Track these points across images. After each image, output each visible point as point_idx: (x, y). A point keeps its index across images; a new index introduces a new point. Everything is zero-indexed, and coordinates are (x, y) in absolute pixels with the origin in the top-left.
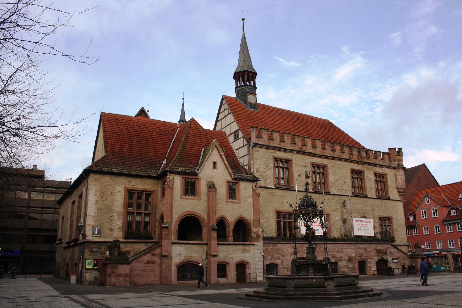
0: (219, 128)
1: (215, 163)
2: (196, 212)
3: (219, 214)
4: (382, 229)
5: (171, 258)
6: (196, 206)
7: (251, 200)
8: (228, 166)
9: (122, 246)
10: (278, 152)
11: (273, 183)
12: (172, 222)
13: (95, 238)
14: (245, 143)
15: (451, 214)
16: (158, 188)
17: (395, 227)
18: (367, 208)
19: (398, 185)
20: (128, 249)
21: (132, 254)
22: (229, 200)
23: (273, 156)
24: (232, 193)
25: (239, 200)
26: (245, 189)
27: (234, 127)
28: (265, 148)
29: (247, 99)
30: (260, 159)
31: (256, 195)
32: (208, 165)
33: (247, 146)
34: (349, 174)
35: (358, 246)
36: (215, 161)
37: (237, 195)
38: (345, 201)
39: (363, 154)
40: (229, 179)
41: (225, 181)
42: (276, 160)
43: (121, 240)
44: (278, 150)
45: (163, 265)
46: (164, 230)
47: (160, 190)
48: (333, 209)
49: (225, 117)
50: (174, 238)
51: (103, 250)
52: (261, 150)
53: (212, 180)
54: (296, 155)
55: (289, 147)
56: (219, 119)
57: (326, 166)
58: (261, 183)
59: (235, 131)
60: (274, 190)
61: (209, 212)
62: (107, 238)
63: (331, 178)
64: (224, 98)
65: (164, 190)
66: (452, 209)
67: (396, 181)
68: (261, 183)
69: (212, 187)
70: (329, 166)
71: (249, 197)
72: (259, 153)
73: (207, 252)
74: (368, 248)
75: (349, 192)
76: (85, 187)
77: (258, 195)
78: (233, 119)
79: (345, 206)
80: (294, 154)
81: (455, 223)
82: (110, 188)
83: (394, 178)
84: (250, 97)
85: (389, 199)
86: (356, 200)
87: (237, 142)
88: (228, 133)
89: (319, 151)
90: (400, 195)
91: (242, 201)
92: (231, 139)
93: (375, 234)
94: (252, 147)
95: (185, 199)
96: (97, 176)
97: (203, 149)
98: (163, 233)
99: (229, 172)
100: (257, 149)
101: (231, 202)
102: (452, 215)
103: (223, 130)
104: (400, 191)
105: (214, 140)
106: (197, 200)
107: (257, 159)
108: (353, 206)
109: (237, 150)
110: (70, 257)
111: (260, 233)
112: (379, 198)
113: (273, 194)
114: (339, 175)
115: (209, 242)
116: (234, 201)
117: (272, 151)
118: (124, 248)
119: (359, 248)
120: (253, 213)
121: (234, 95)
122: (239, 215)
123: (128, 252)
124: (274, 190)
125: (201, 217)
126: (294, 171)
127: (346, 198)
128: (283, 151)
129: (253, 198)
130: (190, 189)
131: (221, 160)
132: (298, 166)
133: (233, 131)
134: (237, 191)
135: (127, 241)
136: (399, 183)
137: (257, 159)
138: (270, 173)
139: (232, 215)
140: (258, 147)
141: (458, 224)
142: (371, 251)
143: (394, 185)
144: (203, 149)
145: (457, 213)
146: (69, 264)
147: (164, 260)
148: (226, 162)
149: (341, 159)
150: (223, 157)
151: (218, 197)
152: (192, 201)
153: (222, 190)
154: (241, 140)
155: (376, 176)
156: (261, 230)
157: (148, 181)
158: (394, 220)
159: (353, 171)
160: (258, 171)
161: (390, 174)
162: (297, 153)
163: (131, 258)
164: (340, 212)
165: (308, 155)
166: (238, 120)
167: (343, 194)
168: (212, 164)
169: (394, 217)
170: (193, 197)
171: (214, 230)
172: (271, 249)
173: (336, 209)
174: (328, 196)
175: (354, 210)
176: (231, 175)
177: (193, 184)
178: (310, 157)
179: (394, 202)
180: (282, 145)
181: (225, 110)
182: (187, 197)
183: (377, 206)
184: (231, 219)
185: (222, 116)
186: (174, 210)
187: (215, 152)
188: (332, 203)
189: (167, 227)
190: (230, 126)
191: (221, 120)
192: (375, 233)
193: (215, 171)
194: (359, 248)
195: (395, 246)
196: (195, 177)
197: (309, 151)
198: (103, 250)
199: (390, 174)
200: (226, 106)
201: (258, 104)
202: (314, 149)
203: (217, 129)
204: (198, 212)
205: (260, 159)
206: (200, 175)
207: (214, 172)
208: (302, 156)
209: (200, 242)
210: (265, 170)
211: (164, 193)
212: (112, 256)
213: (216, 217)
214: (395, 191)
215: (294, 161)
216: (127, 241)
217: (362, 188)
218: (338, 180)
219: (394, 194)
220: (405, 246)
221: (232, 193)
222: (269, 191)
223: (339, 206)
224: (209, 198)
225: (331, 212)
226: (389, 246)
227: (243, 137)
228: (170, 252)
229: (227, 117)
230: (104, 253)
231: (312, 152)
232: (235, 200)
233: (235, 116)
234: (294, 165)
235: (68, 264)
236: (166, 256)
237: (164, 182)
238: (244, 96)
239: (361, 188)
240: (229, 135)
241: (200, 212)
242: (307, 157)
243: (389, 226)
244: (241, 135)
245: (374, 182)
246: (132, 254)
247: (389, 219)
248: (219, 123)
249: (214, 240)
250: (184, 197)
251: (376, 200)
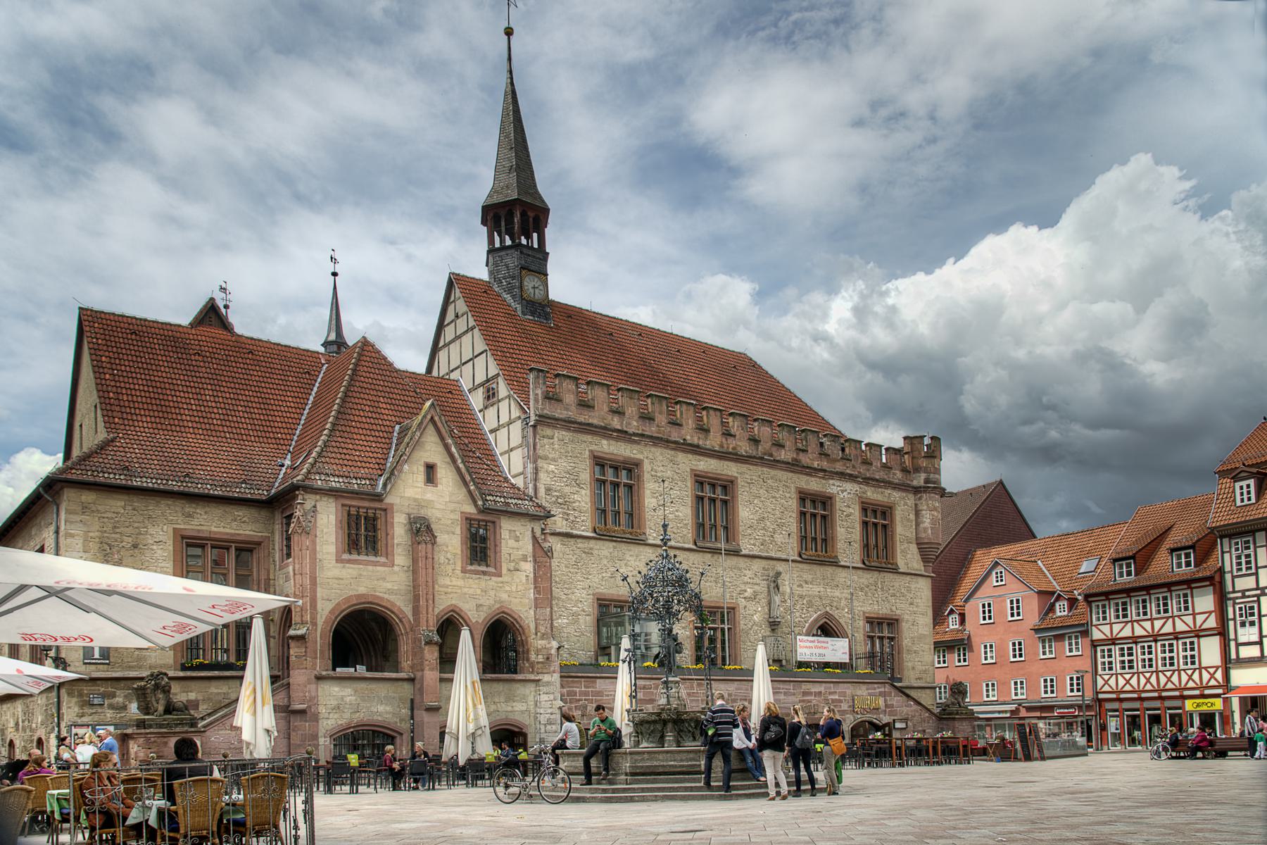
0: (441, 369)
1: (430, 469)
2: (382, 599)
3: (443, 604)
4: (873, 645)
5: (316, 718)
6: (382, 581)
7: (528, 567)
8: (468, 478)
9: (175, 688)
10: (605, 442)
11: (589, 524)
12: (314, 624)
13: (93, 667)
14: (516, 413)
15: (1054, 612)
16: (273, 533)
17: (906, 642)
18: (837, 593)
19: (923, 535)
20: (192, 696)
21: (204, 708)
22: (470, 567)
23: (591, 451)
24: (480, 549)
25: (497, 566)
26: (514, 540)
27: (485, 367)
28: (568, 429)
29: (521, 287)
30: (554, 460)
31: (542, 555)
33: (519, 424)
34: (793, 504)
35: (805, 687)
36: (430, 460)
37: (490, 553)
38: (778, 574)
39: (834, 451)
40: (470, 509)
41: (458, 516)
42: (600, 462)
43: (171, 674)
44: (605, 436)
45: (293, 734)
46: (292, 644)
47: (277, 537)
48: (746, 594)
49: (458, 337)
50: (321, 664)
51: (119, 700)
52: (559, 434)
53: (423, 513)
54: (653, 449)
55: (634, 425)
56: (441, 344)
57: (732, 482)
58: (559, 524)
59: (488, 381)
60: (592, 543)
61: (416, 598)
62: (130, 668)
63: (745, 513)
64: (455, 282)
65: (289, 539)
66: (1059, 598)
67: (917, 525)
68: (559, 524)
69: (421, 530)
70: (740, 482)
71: (525, 559)
72: (555, 442)
73: (412, 701)
74: (830, 693)
75: (792, 551)
76: (52, 528)
77: (549, 553)
78: (480, 346)
79: (777, 587)
80: (648, 448)
81: (1063, 635)
82: (130, 530)
83: (912, 517)
84: (530, 283)
85: (895, 570)
86: (808, 572)
87: (491, 412)
88: (466, 385)
89: (714, 440)
90: (925, 559)
91: (504, 571)
92: (476, 400)
93: (851, 659)
94: (534, 426)
95: (349, 561)
96: (88, 497)
97: (397, 427)
98: (292, 652)
99: (470, 492)
100: (548, 432)
101: (477, 572)
102: (1059, 614)
103: (454, 376)
104: (924, 549)
105: (428, 404)
106: (384, 565)
107: (546, 458)
108: (800, 586)
109: (492, 431)
110: (17, 724)
111: (553, 652)
112: (867, 568)
114: (765, 508)
115: (419, 674)
116: (483, 568)
117: (589, 438)
118: (181, 695)
119: (810, 694)
120: (536, 599)
121: (482, 273)
122: (497, 606)
123: (195, 705)
124: (593, 542)
125: (395, 610)
126: (648, 493)
127: (780, 567)
128: (617, 439)
129: (535, 561)
130: (364, 534)
131: (448, 459)
133: (480, 378)
134: (490, 544)
135: (189, 674)
136: (925, 529)
137: (546, 458)
138: (583, 499)
139: (479, 606)
140: (549, 425)
141: (1070, 638)
142: (841, 701)
143: (911, 534)
144: (397, 427)
145: (1070, 609)
146: (17, 743)
147: (296, 722)
148: (461, 466)
149: (775, 464)
150: (453, 449)
151: (441, 558)
152: (370, 568)
153: (451, 543)
154: (504, 406)
155: (864, 510)
156: (555, 644)
157: (241, 512)
158: (904, 626)
159: (803, 497)
160: (548, 490)
161: (903, 506)
162: (655, 445)
163: (202, 719)
164: (764, 601)
165: (684, 451)
166: (496, 345)
167: (773, 554)
168: (422, 469)
169: (906, 617)
170: (372, 558)
171: (429, 643)
172: (582, 693)
173: (755, 594)
174: (733, 561)
175: (801, 597)
176: (475, 502)
177: (372, 523)
178: (690, 456)
179: (908, 578)
180: (616, 423)
181: (457, 316)
182: (355, 557)
183: (862, 589)
185: (449, 333)
186: (320, 592)
187: (431, 438)
188: (746, 579)
189: (301, 638)
190: (470, 363)
191: (447, 345)
192: (851, 655)
193: (430, 488)
194: (810, 694)
195: (901, 690)
196: (377, 505)
198: (119, 700)
199: (903, 506)
200: (461, 306)
201: (553, 304)
203: (435, 373)
204: (386, 596)
205: (554, 460)
206: (389, 500)
207: (430, 494)
209: (394, 675)
210: (567, 490)
211: (289, 547)
212: (148, 714)
213: (437, 611)
214: (914, 548)
215: (647, 466)
216: (189, 674)
217: (827, 541)
219: (907, 556)
221: (480, 549)
222: (582, 544)
223: (762, 587)
224: (415, 561)
225: (742, 602)
226: (888, 688)
227: (509, 397)
228: (314, 701)
229: (464, 338)
230: (124, 708)
231: (696, 442)
232: (487, 566)
233: (490, 338)
234: (646, 476)
235: (11, 744)
236: (303, 712)
237: (290, 517)
238: (513, 278)
239: (824, 541)
240: (470, 391)
241: (392, 598)
242: (681, 457)
243: (892, 639)
244: (503, 390)
245: (858, 527)
246: (204, 708)
247: (892, 623)
248: (442, 355)
249: (431, 669)
250: (346, 556)
251: (860, 572)
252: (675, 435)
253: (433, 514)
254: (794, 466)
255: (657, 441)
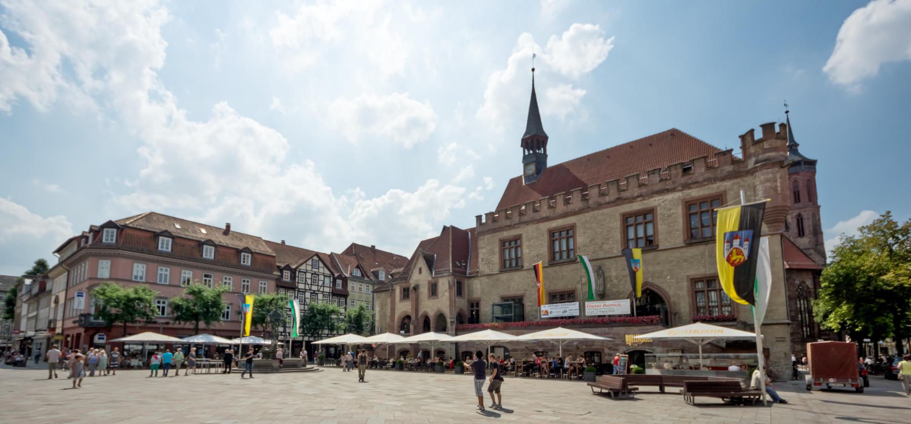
32: (416, 271)
40: (430, 279)
70: (578, 224)
113: (498, 280)
117: (498, 234)
126: (524, 247)
132: (529, 240)
153: (424, 291)
184: (431, 314)
197: (544, 215)
202: (552, 210)
208: (535, 226)
215: (524, 236)
218: (593, 240)
220: (784, 326)
222: (495, 277)
234: (524, 240)
252: (537, 216)
253: (420, 283)
254: (619, 201)
255: (527, 223)
